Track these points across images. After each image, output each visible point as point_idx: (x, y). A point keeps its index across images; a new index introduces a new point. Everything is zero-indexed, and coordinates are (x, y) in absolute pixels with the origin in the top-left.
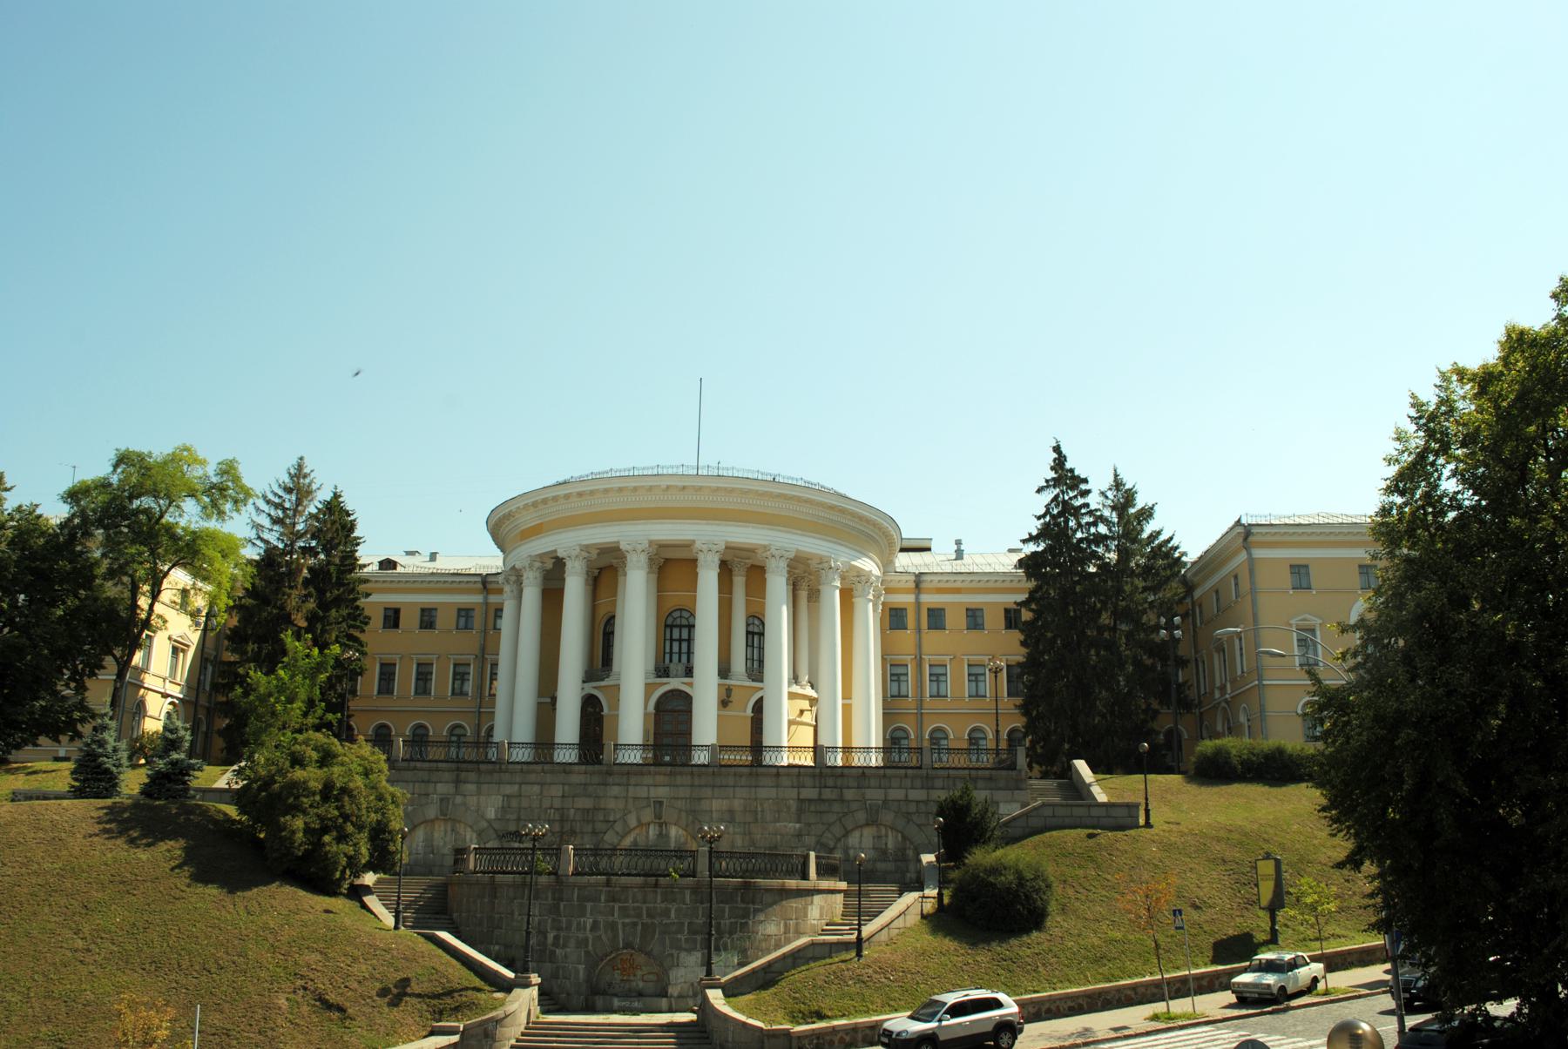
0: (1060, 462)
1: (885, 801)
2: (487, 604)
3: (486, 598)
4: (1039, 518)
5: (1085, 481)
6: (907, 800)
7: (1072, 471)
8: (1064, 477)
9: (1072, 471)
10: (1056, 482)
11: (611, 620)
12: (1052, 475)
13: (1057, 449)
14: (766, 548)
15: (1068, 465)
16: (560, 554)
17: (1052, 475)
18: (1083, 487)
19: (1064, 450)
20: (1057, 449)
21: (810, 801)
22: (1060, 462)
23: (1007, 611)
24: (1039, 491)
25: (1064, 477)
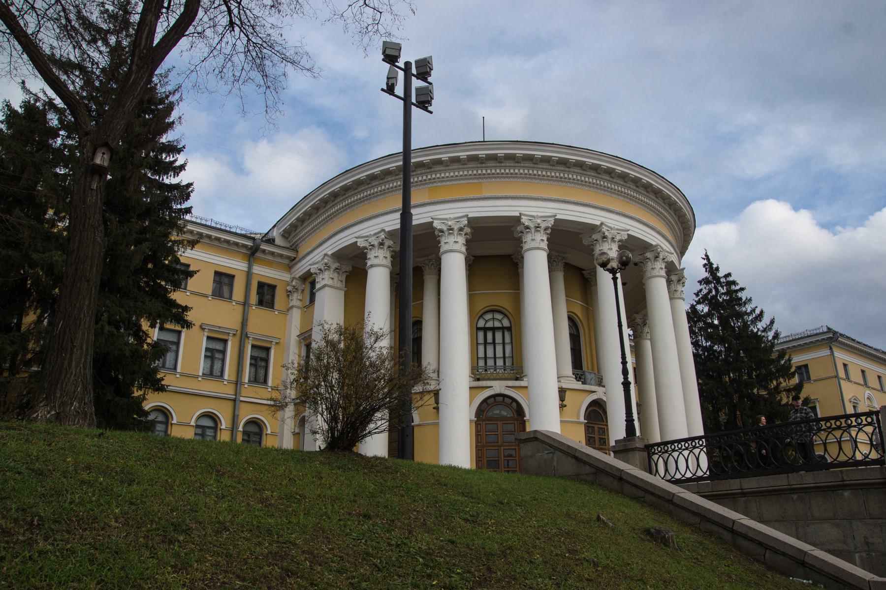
2: (249, 274)
3: (250, 267)
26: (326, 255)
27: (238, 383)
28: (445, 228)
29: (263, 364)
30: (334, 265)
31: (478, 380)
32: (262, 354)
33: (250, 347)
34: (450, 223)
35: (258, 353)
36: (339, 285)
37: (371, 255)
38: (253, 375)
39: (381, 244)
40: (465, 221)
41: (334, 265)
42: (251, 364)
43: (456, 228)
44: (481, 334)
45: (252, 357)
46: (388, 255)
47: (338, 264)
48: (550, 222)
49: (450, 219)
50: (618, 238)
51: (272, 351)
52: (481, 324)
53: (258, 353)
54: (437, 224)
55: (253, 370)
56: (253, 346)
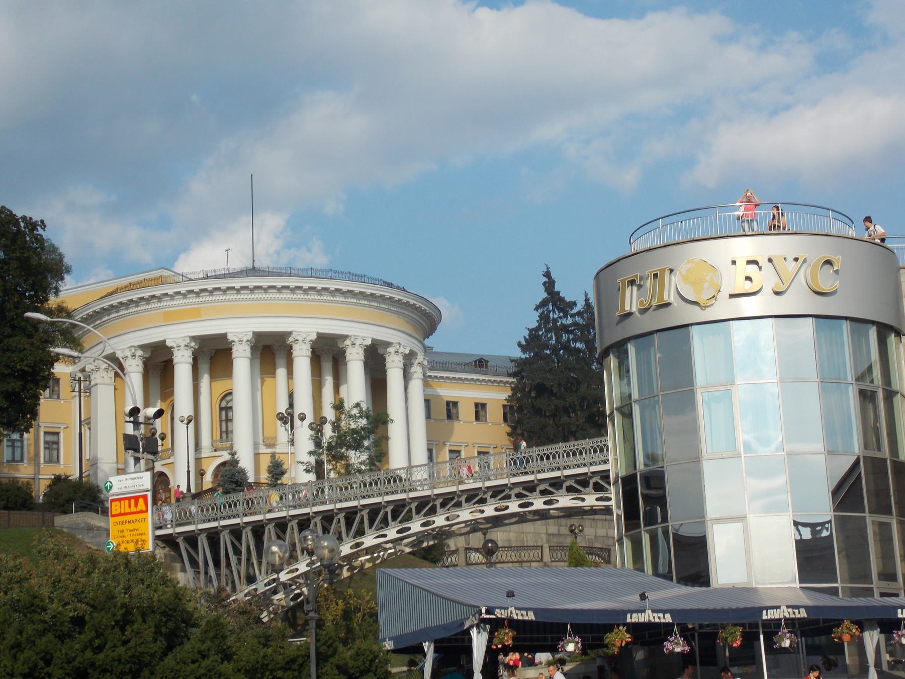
0: (549, 285)
1: (596, 536)
4: (531, 330)
5: (575, 304)
6: (608, 537)
7: (558, 293)
8: (553, 298)
9: (558, 293)
10: (543, 304)
12: (545, 295)
13: (547, 274)
14: (388, 344)
15: (557, 289)
16: (230, 337)
17: (545, 295)
18: (575, 311)
19: (553, 276)
20: (547, 274)
21: (553, 535)
22: (549, 285)
23: (476, 405)
24: (536, 309)
25: (553, 298)
28: (175, 345)
29: (55, 446)
31: (215, 450)
34: (178, 341)
35: (50, 438)
38: (47, 456)
39: (134, 356)
43: (182, 344)
44: (224, 413)
45: (45, 442)
48: (250, 336)
49: (177, 338)
50: (308, 339)
51: (62, 435)
52: (224, 404)
53: (50, 438)
56: (45, 433)
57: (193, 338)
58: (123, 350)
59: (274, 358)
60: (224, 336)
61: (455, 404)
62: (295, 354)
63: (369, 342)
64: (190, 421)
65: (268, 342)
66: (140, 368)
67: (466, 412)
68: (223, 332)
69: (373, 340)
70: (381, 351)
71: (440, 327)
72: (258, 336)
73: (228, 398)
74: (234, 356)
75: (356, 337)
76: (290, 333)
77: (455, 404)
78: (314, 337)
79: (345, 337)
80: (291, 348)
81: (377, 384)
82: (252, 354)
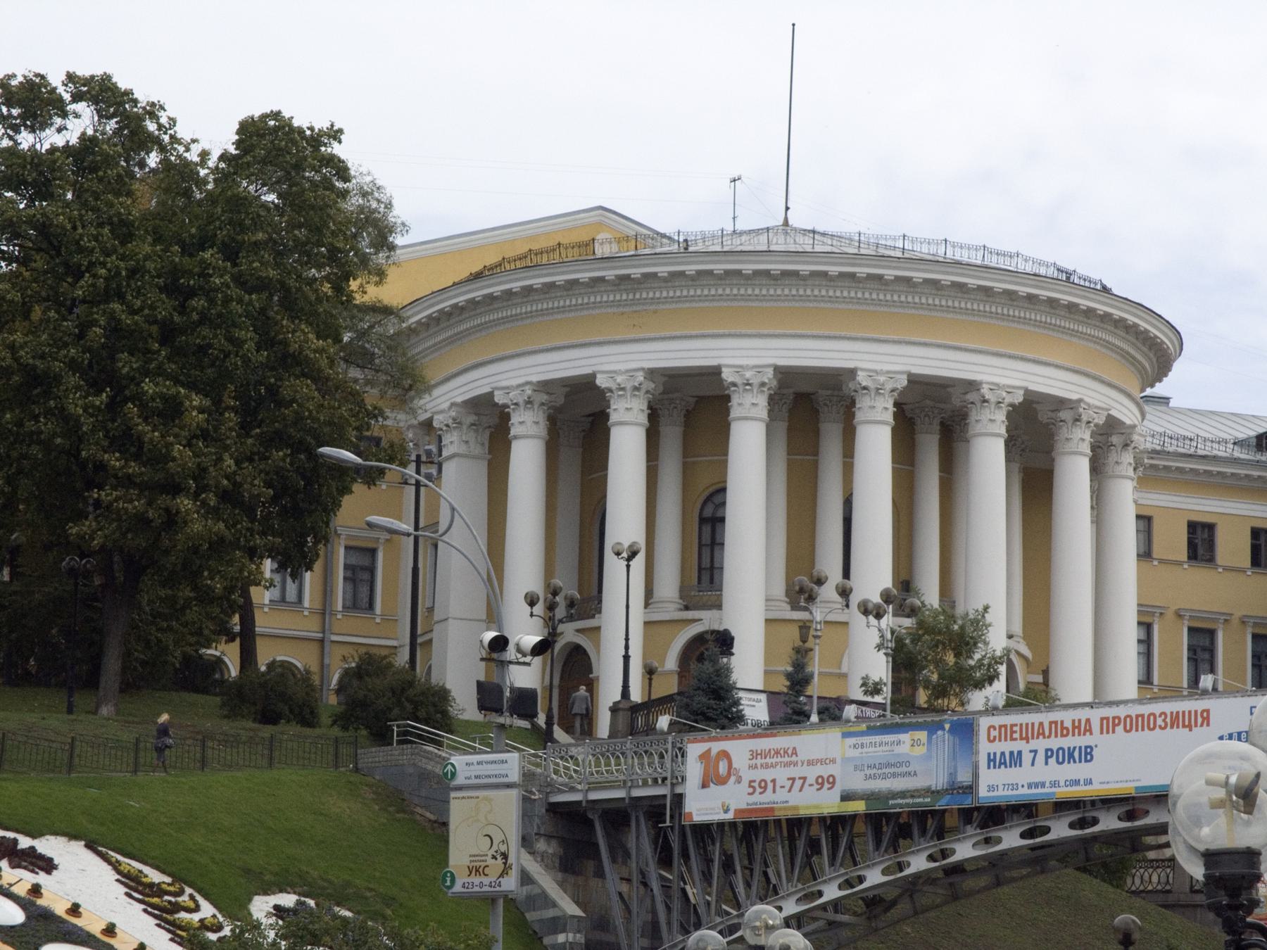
11: (717, 495)
14: (1061, 403)
16: (728, 376)
26: (453, 404)
27: (324, 612)
28: (614, 387)
29: (366, 576)
30: (472, 418)
31: (687, 608)
32: (365, 561)
33: (342, 551)
36: (477, 450)
37: (515, 419)
38: (349, 596)
40: (640, 377)
41: (472, 418)
42: (345, 578)
44: (707, 529)
45: (346, 567)
46: (541, 417)
47: (475, 418)
52: (708, 512)
54: (601, 381)
55: (350, 587)
56: (347, 548)
57: (651, 373)
58: (507, 389)
59: (818, 421)
60: (715, 372)
61: (1210, 528)
62: (860, 416)
63: (1018, 398)
64: (633, 554)
65: (804, 388)
66: (542, 430)
67: (1233, 547)
68: (714, 362)
69: (1027, 392)
70: (1043, 417)
71: (1178, 367)
72: (786, 375)
73: (717, 499)
74: (733, 414)
75: (995, 387)
76: (852, 372)
77: (1210, 528)
78: (903, 382)
79: (972, 385)
80: (853, 403)
81: (1035, 485)
82: (770, 412)
